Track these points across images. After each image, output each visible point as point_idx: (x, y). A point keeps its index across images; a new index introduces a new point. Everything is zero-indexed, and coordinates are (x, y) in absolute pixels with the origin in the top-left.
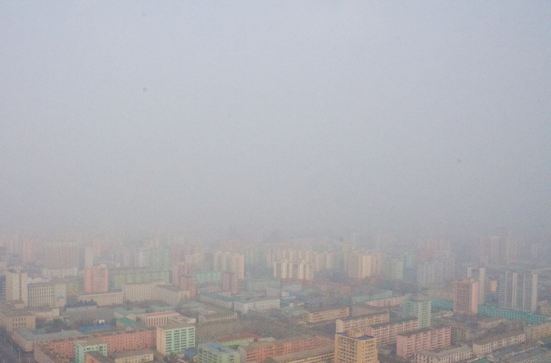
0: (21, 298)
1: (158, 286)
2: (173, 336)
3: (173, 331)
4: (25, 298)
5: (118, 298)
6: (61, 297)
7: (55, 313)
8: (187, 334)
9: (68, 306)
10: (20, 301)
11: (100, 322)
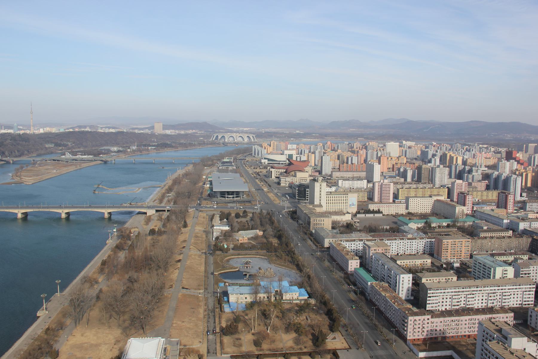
4: (323, 203)
5: (400, 209)
6: (353, 205)
7: (347, 218)
9: (358, 212)
10: (320, 206)
11: (385, 227)
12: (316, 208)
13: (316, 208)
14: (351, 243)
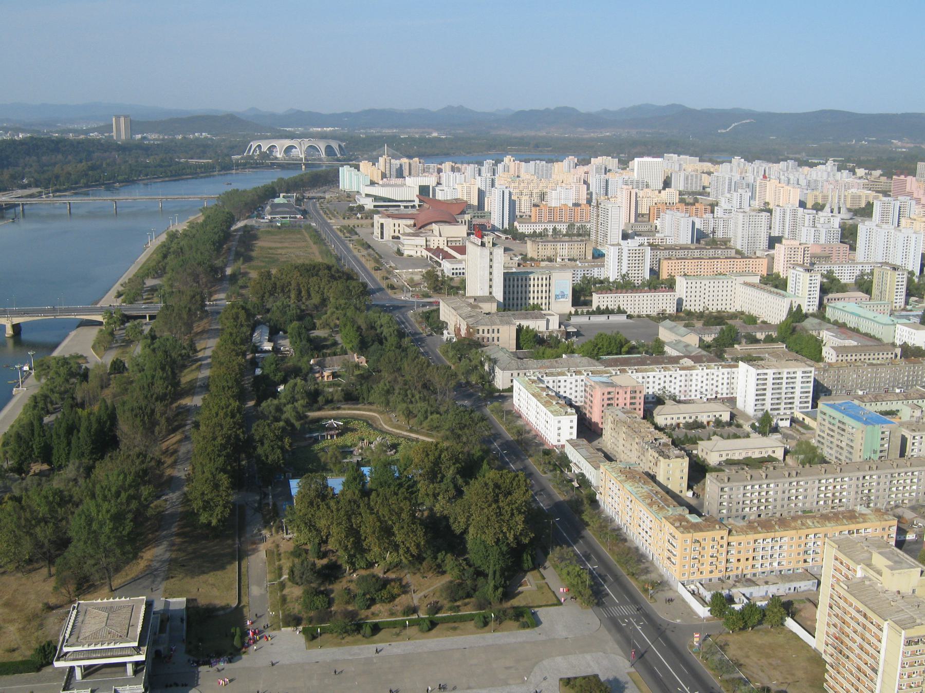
0: (491, 293)
1: (746, 284)
2: (770, 381)
3: (770, 372)
6: (563, 296)
8: (799, 380)
12: (481, 305)
13: (481, 305)
14: (560, 378)
